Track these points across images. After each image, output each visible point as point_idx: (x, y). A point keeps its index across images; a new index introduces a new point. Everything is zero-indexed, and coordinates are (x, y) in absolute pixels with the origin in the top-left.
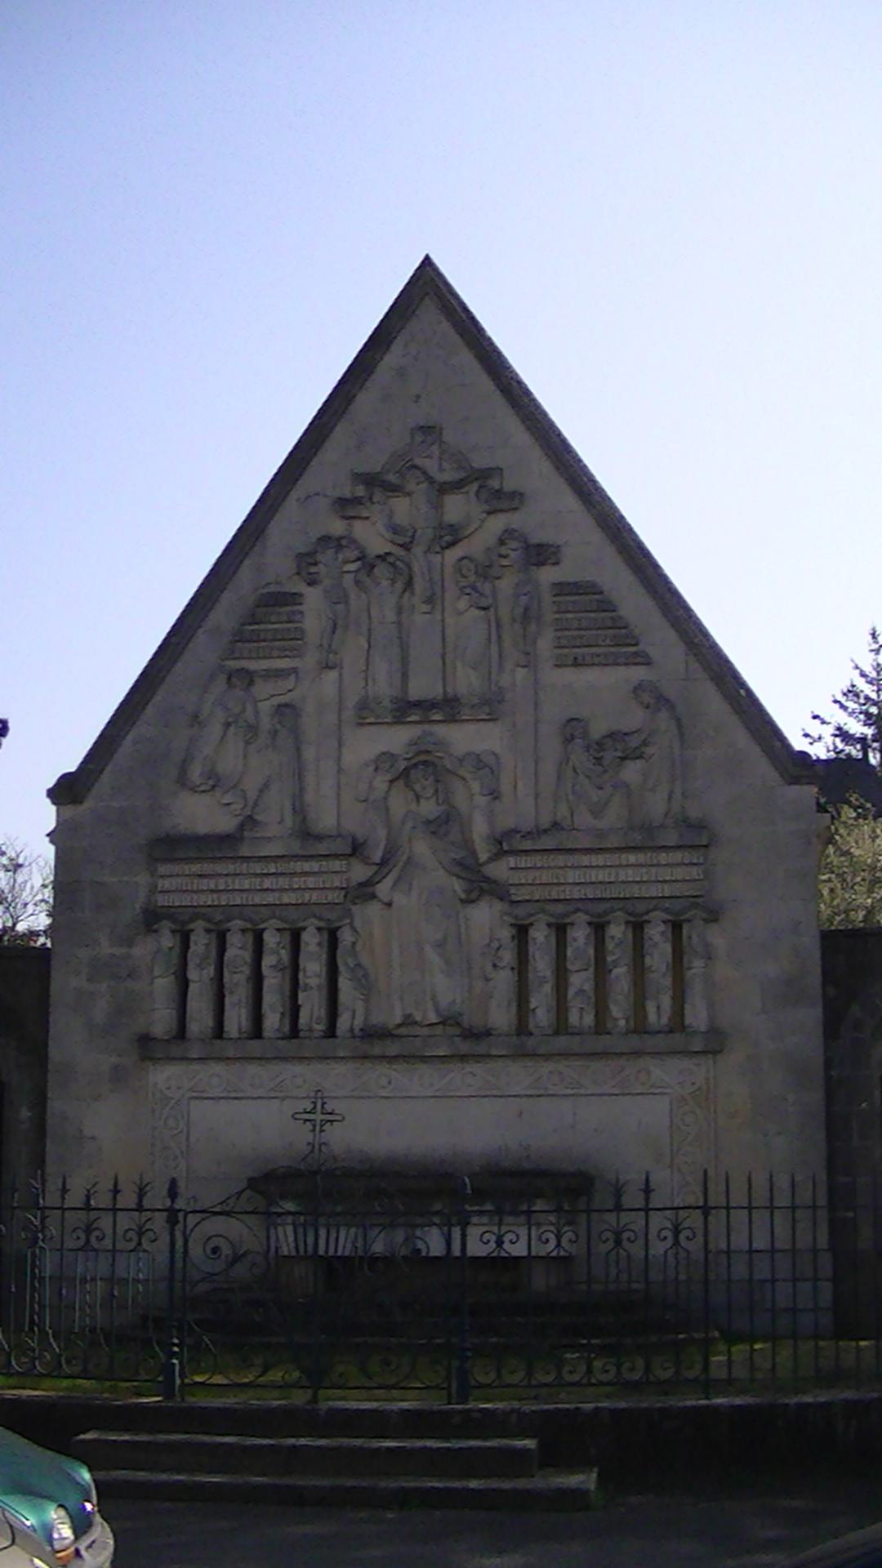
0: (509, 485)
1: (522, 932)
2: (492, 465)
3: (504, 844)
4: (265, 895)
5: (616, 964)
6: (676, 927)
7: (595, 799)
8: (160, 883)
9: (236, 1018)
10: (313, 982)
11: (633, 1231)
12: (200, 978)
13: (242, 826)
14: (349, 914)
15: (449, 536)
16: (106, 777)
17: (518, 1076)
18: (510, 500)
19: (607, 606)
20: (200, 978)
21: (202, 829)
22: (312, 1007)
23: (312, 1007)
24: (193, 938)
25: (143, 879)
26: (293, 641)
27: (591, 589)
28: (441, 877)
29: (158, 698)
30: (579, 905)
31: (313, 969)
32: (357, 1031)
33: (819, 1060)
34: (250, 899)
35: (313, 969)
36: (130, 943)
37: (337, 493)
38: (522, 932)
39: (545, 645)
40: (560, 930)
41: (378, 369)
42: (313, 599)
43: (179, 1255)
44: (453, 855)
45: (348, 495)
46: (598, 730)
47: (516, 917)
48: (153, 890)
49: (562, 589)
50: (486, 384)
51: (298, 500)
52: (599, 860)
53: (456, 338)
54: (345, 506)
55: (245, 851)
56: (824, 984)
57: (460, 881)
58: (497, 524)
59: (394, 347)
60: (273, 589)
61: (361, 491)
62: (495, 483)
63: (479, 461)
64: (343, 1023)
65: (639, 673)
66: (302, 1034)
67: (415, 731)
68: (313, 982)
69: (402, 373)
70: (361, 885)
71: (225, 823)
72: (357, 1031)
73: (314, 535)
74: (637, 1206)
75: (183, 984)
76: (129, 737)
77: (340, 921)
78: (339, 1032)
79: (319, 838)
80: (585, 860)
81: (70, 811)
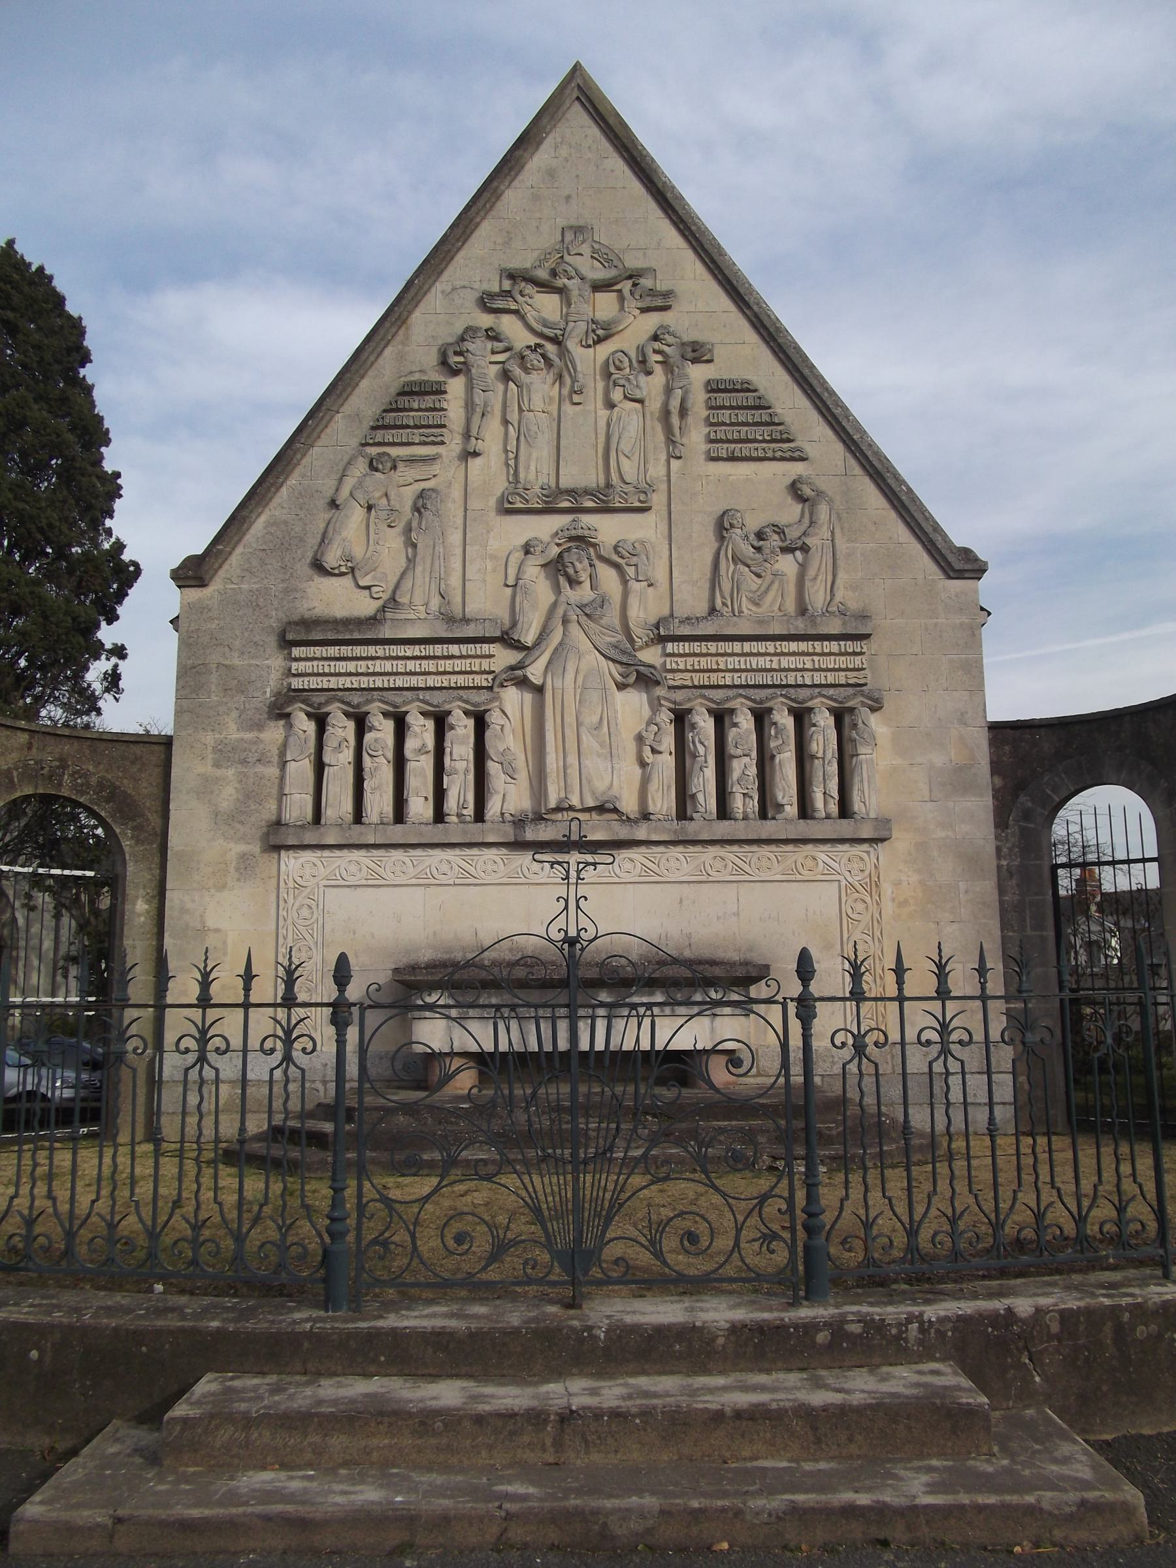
0: (662, 286)
1: (681, 719)
2: (645, 266)
3: (661, 630)
4: (407, 678)
5: (780, 750)
6: (839, 716)
7: (754, 587)
8: (294, 665)
9: (379, 802)
10: (461, 766)
11: (872, 1030)
12: (340, 760)
13: (383, 609)
14: (497, 698)
15: (601, 333)
16: (236, 559)
17: (679, 862)
18: (661, 302)
19: (761, 406)
20: (340, 760)
21: (340, 612)
22: (459, 790)
23: (459, 790)
24: (330, 720)
25: (275, 662)
26: (434, 431)
27: (746, 388)
28: (593, 659)
29: (292, 481)
30: (741, 691)
31: (461, 750)
32: (508, 817)
33: (990, 848)
34: (392, 681)
35: (461, 750)
36: (260, 727)
37: (486, 287)
38: (681, 719)
39: (696, 437)
40: (721, 718)
41: (527, 167)
42: (456, 386)
43: (796, 1054)
44: (609, 639)
45: (496, 289)
46: (753, 523)
47: (675, 703)
48: (289, 673)
49: (713, 387)
50: (636, 187)
51: (443, 292)
52: (761, 647)
53: (605, 144)
54: (486, 303)
55: (387, 632)
56: (993, 773)
57: (618, 666)
58: (652, 321)
59: (544, 147)
60: (416, 377)
61: (507, 285)
62: (646, 282)
63: (633, 262)
64: (493, 808)
65: (797, 469)
66: (447, 819)
67: (563, 520)
68: (461, 766)
69: (551, 174)
70: (512, 668)
71: (365, 606)
72: (508, 817)
73: (459, 328)
74: (999, 994)
75: (320, 767)
76: (263, 519)
77: (487, 704)
78: (488, 817)
79: (466, 620)
80: (747, 647)
81: (194, 594)
